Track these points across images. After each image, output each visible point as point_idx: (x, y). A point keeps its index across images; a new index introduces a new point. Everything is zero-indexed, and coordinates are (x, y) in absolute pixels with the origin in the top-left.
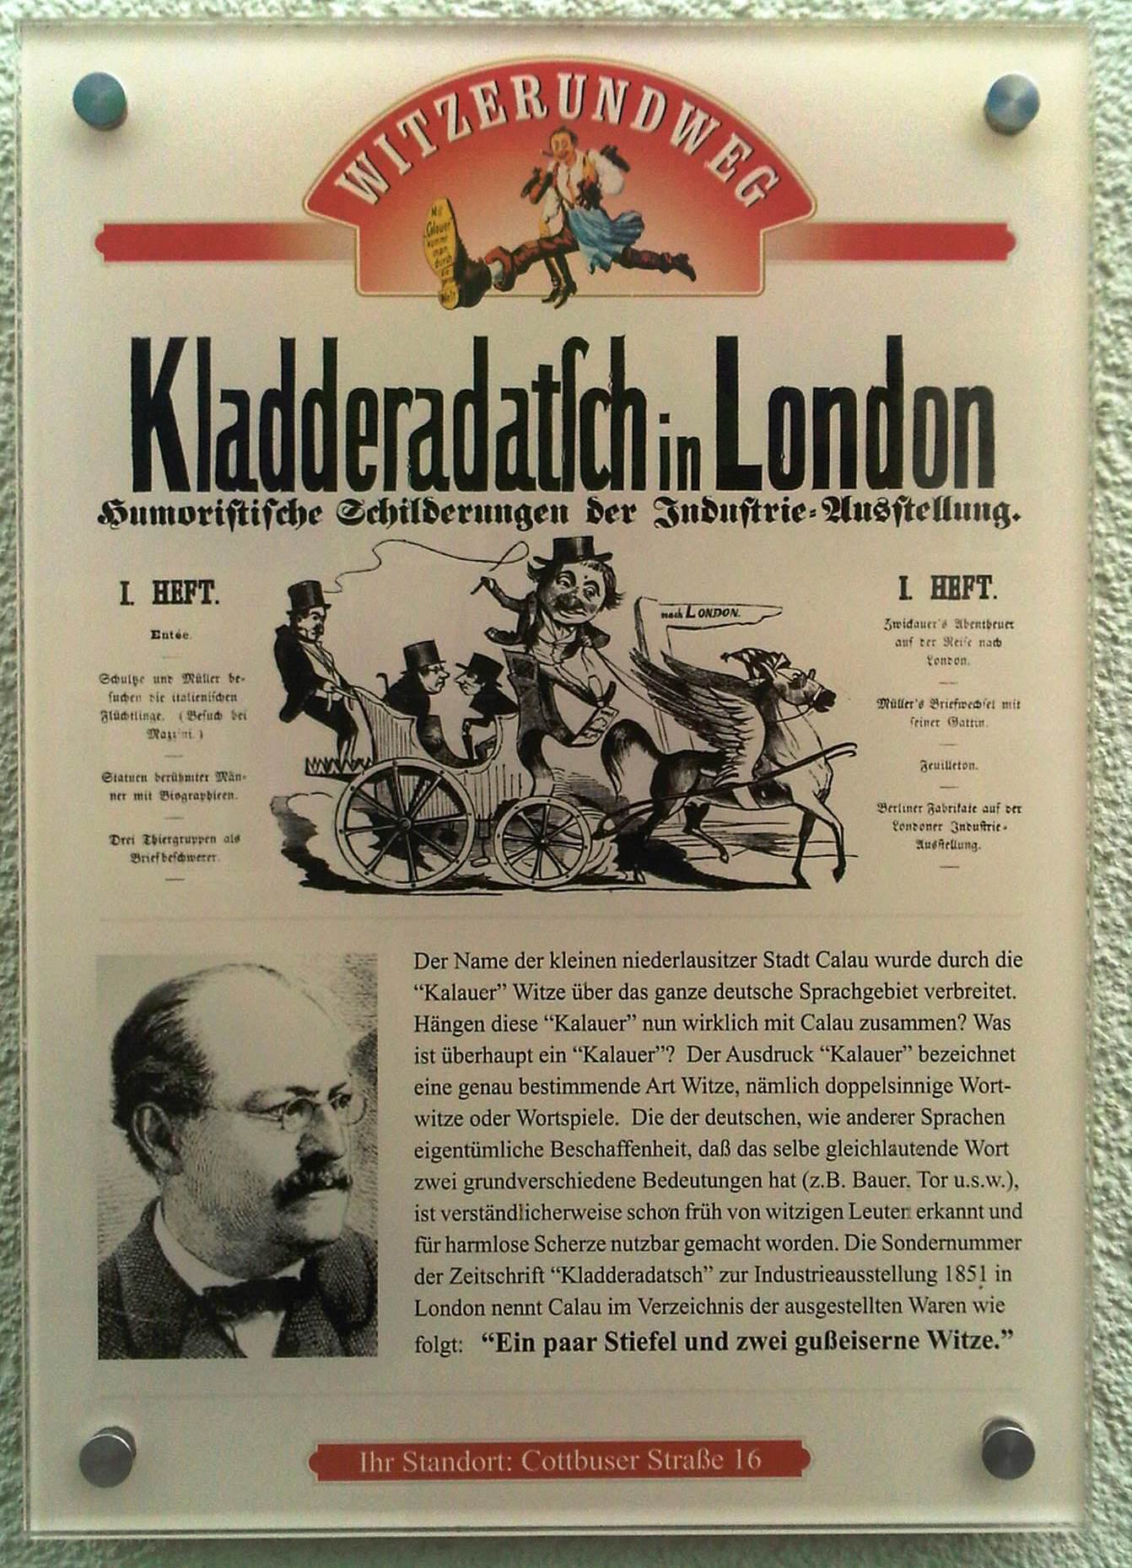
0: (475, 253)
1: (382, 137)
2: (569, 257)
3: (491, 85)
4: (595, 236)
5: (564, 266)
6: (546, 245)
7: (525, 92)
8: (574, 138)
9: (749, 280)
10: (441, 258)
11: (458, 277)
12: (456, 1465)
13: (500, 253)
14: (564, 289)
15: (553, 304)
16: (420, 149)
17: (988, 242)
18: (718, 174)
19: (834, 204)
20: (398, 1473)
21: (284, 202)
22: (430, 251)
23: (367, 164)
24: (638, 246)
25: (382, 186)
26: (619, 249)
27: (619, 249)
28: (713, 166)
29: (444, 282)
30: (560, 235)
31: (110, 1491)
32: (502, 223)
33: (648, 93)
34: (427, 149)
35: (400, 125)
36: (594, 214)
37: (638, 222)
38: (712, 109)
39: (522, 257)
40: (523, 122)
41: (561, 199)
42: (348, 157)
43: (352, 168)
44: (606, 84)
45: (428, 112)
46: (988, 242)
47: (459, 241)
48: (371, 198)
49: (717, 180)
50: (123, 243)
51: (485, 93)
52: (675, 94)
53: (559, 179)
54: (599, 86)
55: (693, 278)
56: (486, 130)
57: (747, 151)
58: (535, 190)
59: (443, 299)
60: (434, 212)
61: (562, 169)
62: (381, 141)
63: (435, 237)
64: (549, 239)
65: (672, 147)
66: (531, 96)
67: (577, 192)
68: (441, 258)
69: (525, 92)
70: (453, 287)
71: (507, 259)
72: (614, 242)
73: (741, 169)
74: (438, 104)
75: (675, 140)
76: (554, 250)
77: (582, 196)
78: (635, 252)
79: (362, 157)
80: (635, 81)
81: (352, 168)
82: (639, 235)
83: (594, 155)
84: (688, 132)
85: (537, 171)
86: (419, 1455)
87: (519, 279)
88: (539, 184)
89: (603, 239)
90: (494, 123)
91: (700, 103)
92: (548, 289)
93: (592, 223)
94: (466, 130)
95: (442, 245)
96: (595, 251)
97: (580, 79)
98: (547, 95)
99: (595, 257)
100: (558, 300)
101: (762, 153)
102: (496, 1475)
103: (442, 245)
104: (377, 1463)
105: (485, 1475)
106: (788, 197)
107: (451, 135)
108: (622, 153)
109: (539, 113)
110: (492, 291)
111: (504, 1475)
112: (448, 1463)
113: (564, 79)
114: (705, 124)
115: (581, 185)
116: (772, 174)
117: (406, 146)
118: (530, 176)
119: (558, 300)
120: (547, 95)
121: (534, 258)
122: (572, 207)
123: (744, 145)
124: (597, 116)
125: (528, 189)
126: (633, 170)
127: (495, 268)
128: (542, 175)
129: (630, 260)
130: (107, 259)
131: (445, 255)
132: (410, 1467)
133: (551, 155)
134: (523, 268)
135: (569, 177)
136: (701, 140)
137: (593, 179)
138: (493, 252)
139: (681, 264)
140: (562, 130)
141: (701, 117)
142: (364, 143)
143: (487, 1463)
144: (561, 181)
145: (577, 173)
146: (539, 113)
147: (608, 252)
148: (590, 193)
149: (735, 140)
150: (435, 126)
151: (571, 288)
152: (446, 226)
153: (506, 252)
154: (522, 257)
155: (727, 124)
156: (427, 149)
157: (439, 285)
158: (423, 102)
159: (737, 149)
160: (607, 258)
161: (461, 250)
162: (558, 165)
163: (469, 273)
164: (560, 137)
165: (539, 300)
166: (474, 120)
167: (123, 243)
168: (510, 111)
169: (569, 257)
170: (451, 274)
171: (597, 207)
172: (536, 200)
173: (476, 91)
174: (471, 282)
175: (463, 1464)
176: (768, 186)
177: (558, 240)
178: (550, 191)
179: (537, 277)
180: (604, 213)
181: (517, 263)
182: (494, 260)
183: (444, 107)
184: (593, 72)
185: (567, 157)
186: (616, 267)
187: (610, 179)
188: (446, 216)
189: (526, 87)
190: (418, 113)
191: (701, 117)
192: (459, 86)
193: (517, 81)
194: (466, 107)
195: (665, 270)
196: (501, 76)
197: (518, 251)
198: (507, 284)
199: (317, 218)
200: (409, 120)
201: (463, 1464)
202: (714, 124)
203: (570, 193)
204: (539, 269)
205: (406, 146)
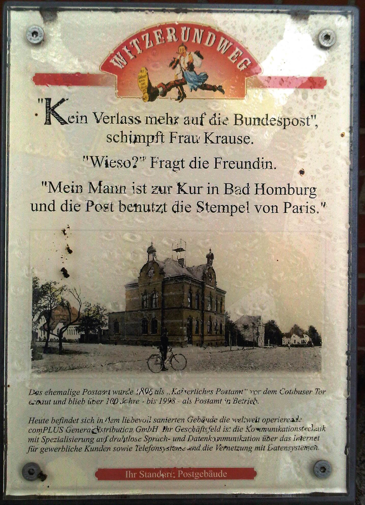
0: (154, 85)
4: (191, 79)
5: (182, 89)
6: (177, 83)
8: (186, 48)
9: (241, 94)
10: (143, 86)
11: (148, 92)
13: (162, 85)
14: (182, 97)
15: (178, 102)
16: (137, 51)
20: (138, 478)
21: (93, 67)
22: (140, 84)
23: (120, 55)
24: (206, 82)
28: (230, 58)
29: (144, 94)
32: (162, 75)
33: (210, 34)
34: (139, 51)
37: (206, 76)
39: (169, 86)
41: (181, 68)
44: (197, 31)
47: (149, 81)
49: (231, 62)
51: (158, 33)
52: (219, 35)
54: (194, 31)
56: (158, 45)
58: (174, 64)
59: (144, 99)
60: (141, 71)
61: (182, 58)
62: (125, 49)
63: (141, 80)
64: (178, 81)
67: (187, 65)
71: (164, 87)
72: (199, 82)
74: (143, 37)
75: (218, 49)
76: (179, 84)
79: (118, 53)
80: (206, 30)
83: (192, 53)
84: (222, 47)
85: (174, 58)
87: (168, 93)
88: (174, 64)
92: (177, 96)
93: (192, 76)
94: (152, 45)
96: (192, 84)
97: (189, 29)
98: (178, 34)
99: (192, 86)
100: (181, 99)
107: (147, 47)
108: (201, 53)
110: (159, 96)
112: (154, 475)
113: (184, 29)
114: (228, 44)
115: (188, 63)
117: (132, 50)
119: (181, 99)
121: (173, 86)
123: (240, 51)
124: (194, 41)
125: (171, 64)
127: (160, 89)
130: (36, 84)
132: (142, 476)
133: (179, 53)
134: (169, 90)
135: (184, 61)
136: (226, 50)
141: (227, 42)
142: (119, 49)
144: (182, 62)
145: (187, 60)
147: (196, 85)
148: (191, 67)
150: (142, 44)
151: (185, 96)
152: (145, 76)
153: (164, 84)
154: (169, 86)
156: (139, 51)
157: (143, 95)
158: (138, 36)
162: (181, 57)
163: (152, 91)
164: (182, 48)
165: (174, 100)
167: (41, 79)
173: (155, 32)
174: (152, 94)
176: (247, 64)
177: (180, 81)
178: (178, 65)
179: (174, 92)
180: (195, 72)
181: (167, 88)
182: (160, 87)
183: (145, 37)
184: (192, 27)
185: (183, 54)
186: (199, 90)
187: (197, 61)
189: (171, 31)
190: (137, 39)
191: (227, 42)
192: (150, 31)
193: (168, 29)
194: (152, 38)
195: (215, 90)
196: (163, 27)
197: (168, 84)
198: (164, 94)
199: (104, 73)
200: (134, 41)
203: (185, 66)
205: (132, 50)
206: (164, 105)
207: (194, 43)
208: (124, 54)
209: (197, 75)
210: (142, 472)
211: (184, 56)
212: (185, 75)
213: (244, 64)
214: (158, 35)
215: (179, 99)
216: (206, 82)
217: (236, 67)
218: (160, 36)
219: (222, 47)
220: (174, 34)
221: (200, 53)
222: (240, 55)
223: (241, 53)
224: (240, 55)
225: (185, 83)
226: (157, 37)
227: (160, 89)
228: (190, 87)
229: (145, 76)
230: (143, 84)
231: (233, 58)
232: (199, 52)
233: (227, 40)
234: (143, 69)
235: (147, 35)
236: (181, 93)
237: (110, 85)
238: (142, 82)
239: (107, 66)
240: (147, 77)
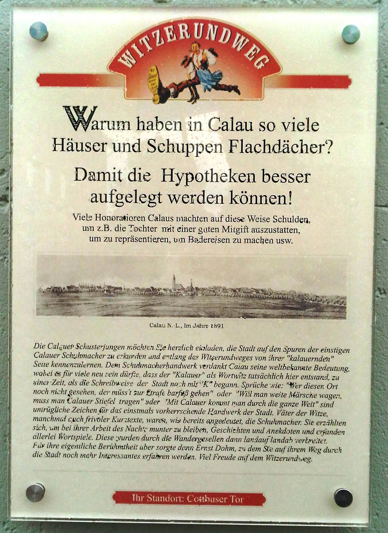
0: (165, 85)
1: (134, 45)
2: (196, 86)
3: (171, 27)
4: (205, 79)
6: (190, 82)
7: (183, 30)
8: (199, 45)
9: (259, 95)
10: (154, 86)
11: (159, 93)
13: (173, 85)
14: (195, 97)
17: (342, 82)
18: (248, 58)
19: (288, 69)
22: (150, 84)
24: (221, 83)
25: (134, 62)
26: (214, 84)
27: (214, 84)
28: (247, 55)
29: (154, 95)
30: (194, 79)
31: (43, 499)
32: (174, 74)
33: (225, 30)
34: (149, 48)
35: (140, 41)
36: (206, 72)
37: (221, 74)
39: (181, 87)
41: (194, 66)
42: (123, 51)
44: (210, 26)
45: (150, 36)
46: (342, 82)
47: (160, 81)
48: (130, 66)
49: (248, 60)
50: (46, 80)
51: (169, 30)
52: (234, 30)
53: (194, 59)
54: (208, 27)
55: (239, 94)
57: (259, 50)
58: (186, 63)
59: (154, 100)
61: (195, 56)
62: (134, 46)
63: (151, 79)
64: (190, 80)
65: (232, 48)
66: (185, 31)
67: (200, 64)
68: (154, 86)
69: (183, 30)
70: (157, 97)
71: (176, 87)
72: (213, 81)
73: (256, 56)
75: (234, 46)
76: (192, 84)
77: (202, 65)
80: (220, 26)
81: (124, 55)
82: (221, 79)
83: (206, 51)
84: (238, 44)
87: (180, 94)
91: (243, 33)
92: (190, 97)
94: (163, 42)
95: (154, 82)
96: (206, 84)
97: (202, 25)
98: (190, 31)
99: (206, 86)
101: (264, 51)
103: (154, 82)
106: (273, 66)
107: (158, 45)
108: (216, 51)
113: (196, 25)
114: (244, 41)
115: (201, 62)
116: (267, 58)
117: (142, 48)
120: (190, 31)
121: (185, 87)
122: (198, 69)
124: (207, 38)
125: (183, 63)
126: (219, 56)
127: (172, 90)
129: (218, 87)
131: (155, 86)
133: (192, 51)
134: (181, 90)
135: (198, 59)
137: (205, 59)
140: (195, 42)
141: (243, 38)
142: (128, 47)
144: (195, 60)
145: (200, 58)
146: (187, 36)
147: (210, 85)
148: (205, 64)
149: (254, 46)
150: (152, 42)
151: (198, 97)
153: (176, 85)
155: (252, 41)
156: (149, 48)
157: (153, 96)
158: (148, 33)
159: (255, 50)
162: (194, 55)
163: (163, 92)
164: (195, 45)
165: (186, 101)
166: (165, 39)
167: (46, 80)
168: (178, 36)
169: (196, 86)
170: (157, 92)
174: (163, 95)
176: (266, 62)
177: (193, 81)
178: (191, 64)
179: (186, 93)
180: (209, 71)
181: (179, 88)
183: (155, 35)
184: (206, 22)
185: (197, 52)
186: (213, 90)
187: (212, 59)
188: (155, 72)
189: (183, 27)
190: (146, 37)
191: (243, 38)
192: (161, 27)
193: (180, 26)
194: (163, 34)
195: (230, 91)
196: (175, 24)
198: (176, 96)
199: (112, 73)
200: (144, 39)
202: (247, 40)
203: (198, 64)
204: (187, 90)
205: (142, 48)
206: (177, 107)
207: (207, 40)
208: (133, 52)
209: (212, 75)
213: (261, 62)
216: (221, 83)
217: (254, 64)
218: (171, 33)
220: (187, 31)
222: (257, 52)
224: (257, 52)
226: (168, 34)
227: (172, 90)
231: (250, 56)
232: (213, 49)
234: (154, 68)
235: (158, 32)
237: (119, 85)
239: (115, 65)
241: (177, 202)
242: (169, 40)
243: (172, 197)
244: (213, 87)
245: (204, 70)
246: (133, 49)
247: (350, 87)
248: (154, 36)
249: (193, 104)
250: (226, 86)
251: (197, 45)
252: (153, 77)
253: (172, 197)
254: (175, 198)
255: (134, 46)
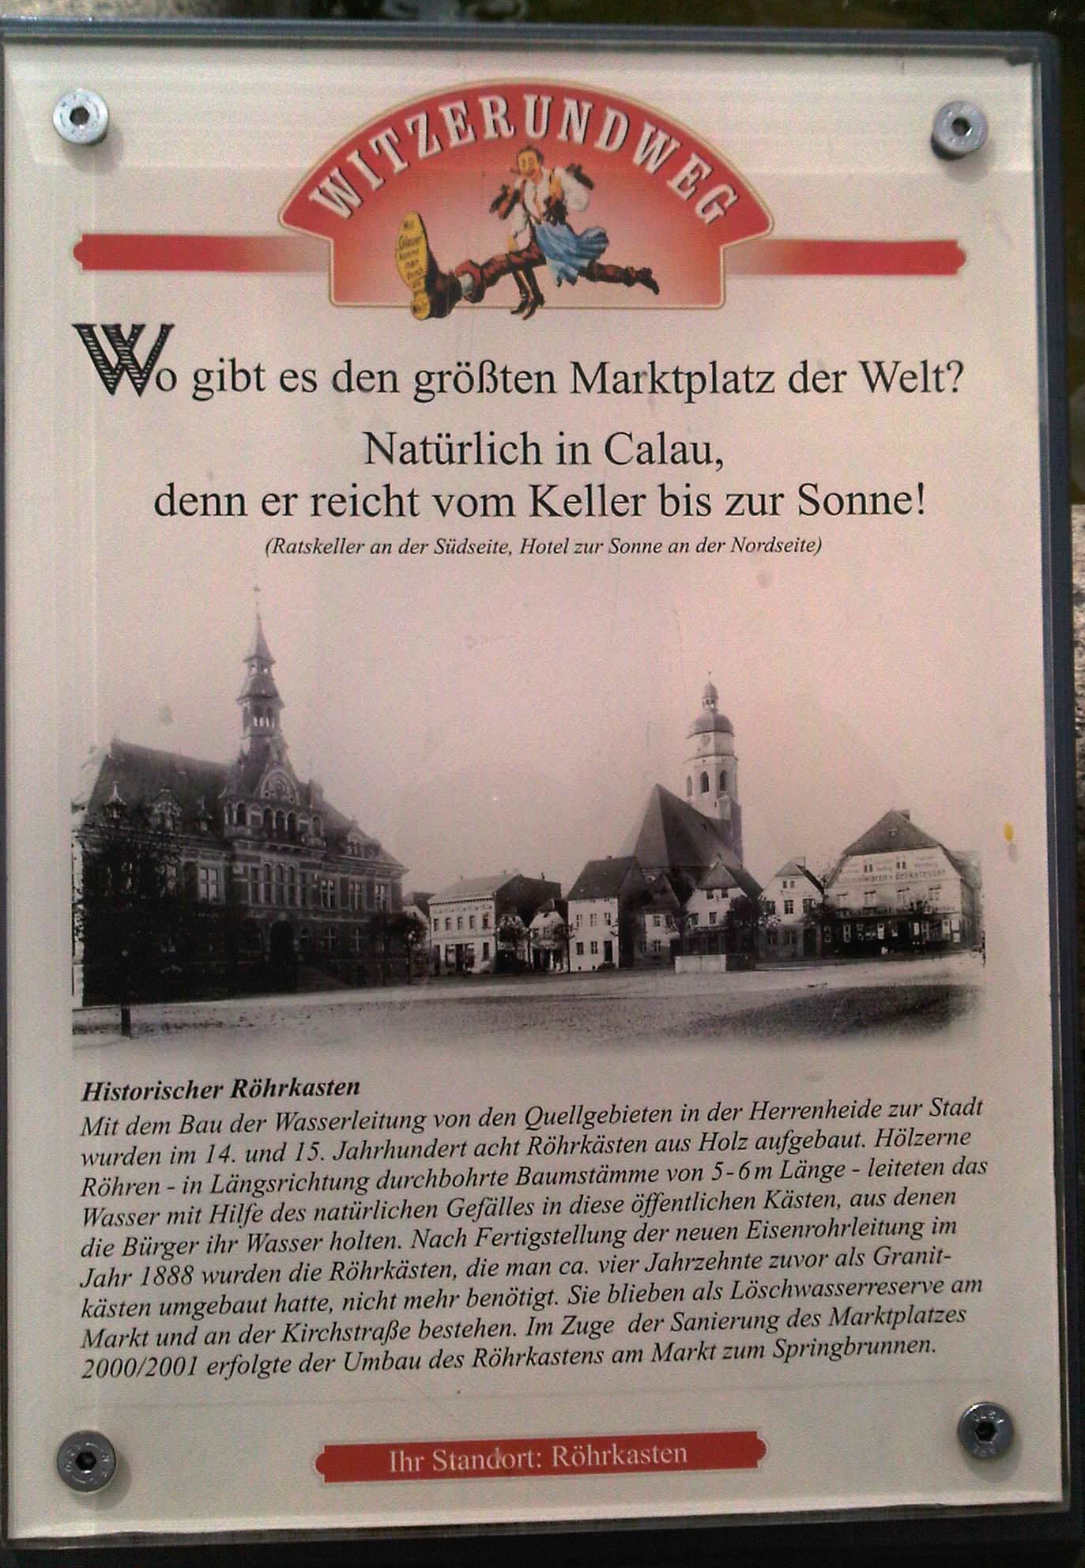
0: (446, 266)
2: (538, 271)
3: (460, 106)
4: (560, 251)
6: (518, 260)
8: (540, 157)
9: (710, 293)
10: (413, 270)
12: (485, 1462)
13: (470, 266)
14: (532, 301)
15: (519, 317)
16: (391, 166)
17: (940, 258)
20: (428, 1472)
21: (259, 218)
22: (402, 264)
24: (604, 260)
25: (355, 201)
26: (585, 263)
28: (673, 184)
29: (416, 294)
30: (528, 249)
32: (473, 237)
33: (611, 115)
34: (398, 165)
36: (561, 230)
37: (602, 238)
38: (673, 131)
39: (491, 270)
40: (491, 141)
41: (528, 215)
43: (326, 184)
44: (571, 105)
45: (399, 130)
46: (940, 258)
48: (345, 212)
49: (677, 197)
50: (100, 252)
52: (637, 116)
54: (563, 106)
55: (656, 291)
56: (456, 148)
57: (707, 170)
58: (504, 206)
60: (406, 226)
61: (530, 185)
62: (354, 158)
63: (405, 251)
64: (518, 254)
65: (634, 166)
66: (499, 116)
67: (544, 209)
68: (413, 270)
70: (424, 299)
71: (478, 275)
73: (701, 187)
74: (409, 123)
75: (638, 159)
76: (522, 264)
77: (549, 212)
78: (600, 266)
79: (335, 173)
80: (599, 102)
81: (326, 184)
82: (603, 251)
83: (560, 172)
84: (650, 153)
85: (505, 188)
86: (448, 1454)
87: (489, 291)
88: (506, 201)
89: (570, 254)
90: (463, 142)
91: (660, 124)
92: (516, 300)
93: (558, 238)
94: (436, 148)
95: (413, 258)
96: (562, 265)
97: (546, 101)
98: (514, 115)
100: (526, 311)
101: (721, 172)
102: (525, 1471)
103: (413, 258)
104: (406, 1463)
105: (508, 1472)
106: (746, 215)
107: (422, 152)
109: (506, 133)
110: (463, 302)
111: (534, 1472)
112: (478, 1461)
114: (666, 145)
115: (547, 201)
116: (731, 192)
117: (378, 163)
118: (498, 193)
119: (526, 311)
120: (514, 115)
122: (539, 222)
123: (702, 163)
125: (496, 205)
126: (597, 187)
127: (466, 281)
128: (510, 192)
129: (597, 273)
131: (416, 268)
132: (440, 1465)
133: (519, 173)
134: (492, 281)
135: (536, 195)
137: (559, 196)
138: (462, 265)
139: (645, 278)
140: (529, 148)
142: (338, 159)
143: (517, 1460)
144: (528, 196)
145: (544, 190)
146: (506, 133)
148: (556, 210)
149: (694, 160)
150: (405, 145)
151: (539, 300)
152: (417, 240)
155: (688, 145)
156: (398, 165)
158: (394, 121)
159: (697, 168)
160: (573, 272)
161: (432, 263)
162: (525, 182)
163: (440, 285)
164: (528, 155)
165: (508, 311)
166: (443, 140)
167: (100, 252)
168: (479, 130)
169: (538, 271)
170: (423, 285)
171: (563, 222)
172: (505, 216)
173: (446, 110)
174: (441, 294)
175: (493, 1462)
176: (727, 205)
177: (525, 254)
178: (518, 207)
179: (506, 290)
180: (570, 229)
181: (485, 276)
182: (464, 273)
183: (415, 125)
184: (558, 94)
186: (582, 280)
187: (575, 195)
188: (416, 231)
189: (494, 108)
190: (390, 132)
192: (430, 106)
193: (485, 102)
194: (436, 125)
196: (469, 97)
197: (488, 264)
198: (477, 295)
201: (493, 1462)
202: (674, 144)
203: (537, 209)
204: (507, 281)
205: (378, 163)
208: (351, 176)
209: (577, 237)
210: (440, 1455)
211: (536, 181)
212: (538, 233)
214: (455, 119)
215: (521, 308)
217: (695, 205)
219: (650, 153)
221: (583, 171)
223: (707, 170)
225: (541, 261)
228: (556, 274)
229: (417, 240)
230: (413, 264)
232: (580, 168)
233: (664, 131)
234: (412, 218)
236: (527, 293)
238: (409, 260)
239: (302, 211)
240: (423, 241)
241: (888, 386)
242: (454, 140)
243: (873, 371)
244: (583, 272)
245: (554, 224)
246: (352, 166)
247: (965, 271)
248: (410, 130)
249: (525, 318)
250: (618, 268)
251: (535, 157)
252: (409, 243)
253: (873, 371)
254: (881, 372)
255: (354, 158)
